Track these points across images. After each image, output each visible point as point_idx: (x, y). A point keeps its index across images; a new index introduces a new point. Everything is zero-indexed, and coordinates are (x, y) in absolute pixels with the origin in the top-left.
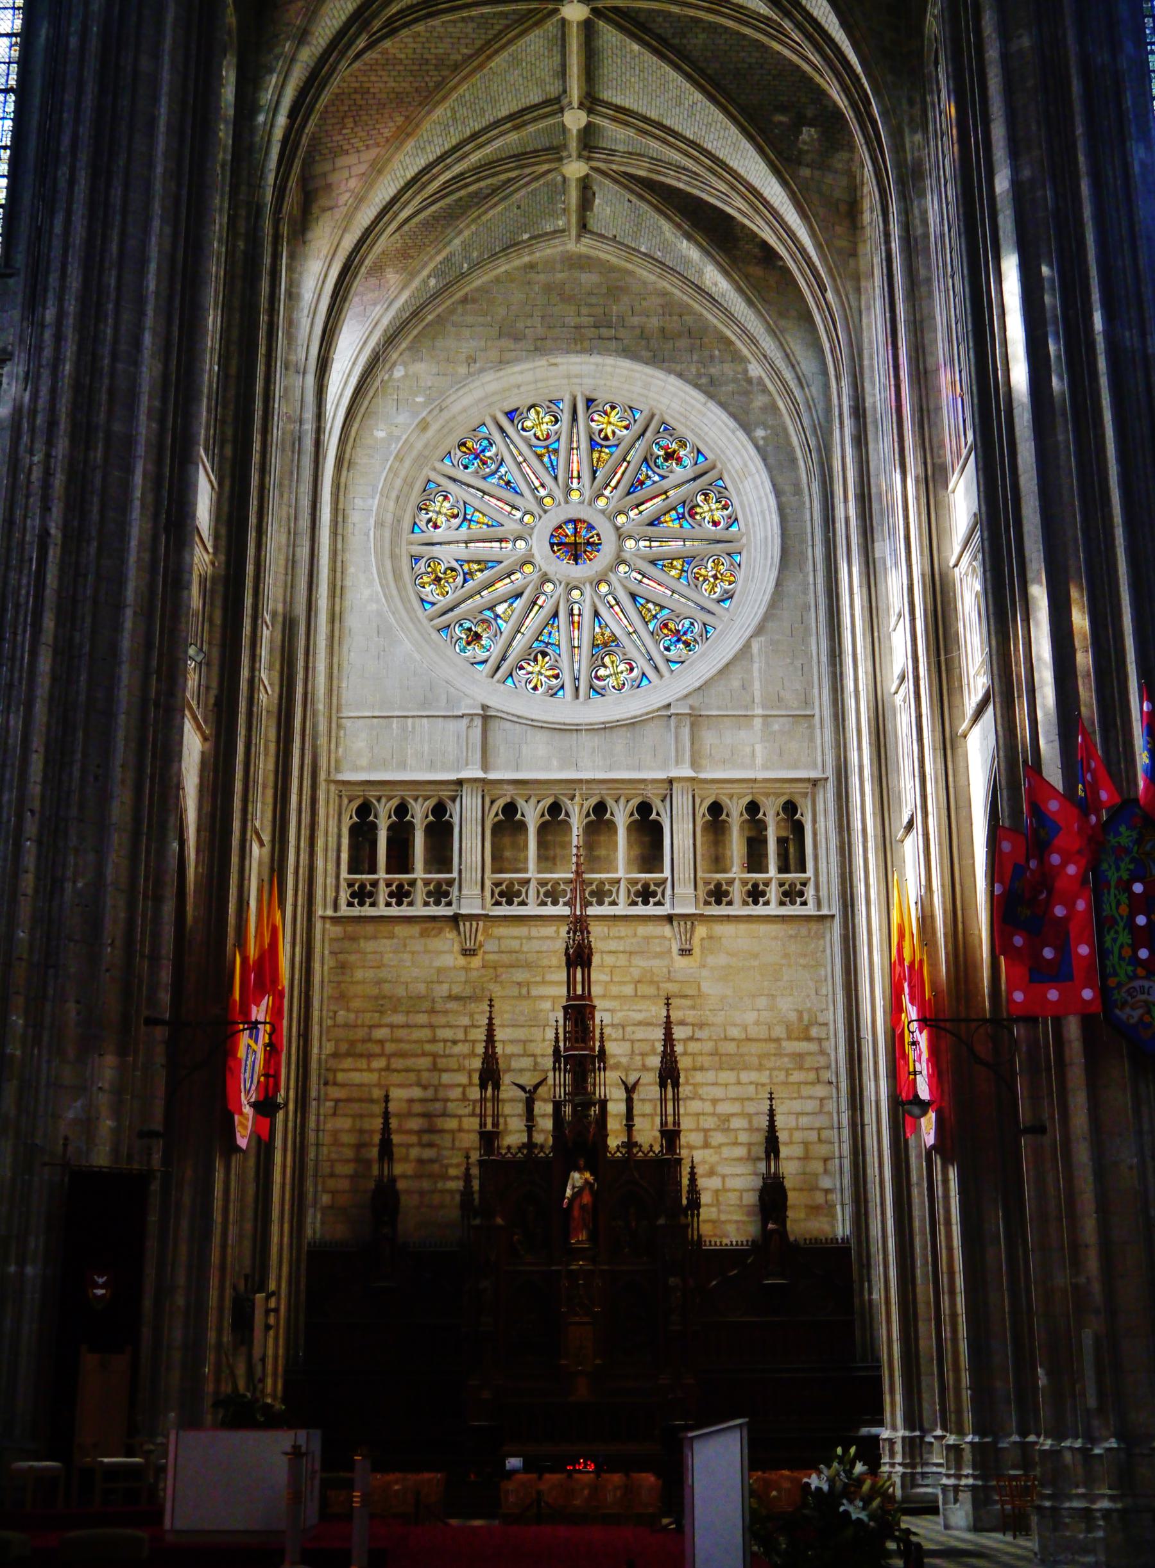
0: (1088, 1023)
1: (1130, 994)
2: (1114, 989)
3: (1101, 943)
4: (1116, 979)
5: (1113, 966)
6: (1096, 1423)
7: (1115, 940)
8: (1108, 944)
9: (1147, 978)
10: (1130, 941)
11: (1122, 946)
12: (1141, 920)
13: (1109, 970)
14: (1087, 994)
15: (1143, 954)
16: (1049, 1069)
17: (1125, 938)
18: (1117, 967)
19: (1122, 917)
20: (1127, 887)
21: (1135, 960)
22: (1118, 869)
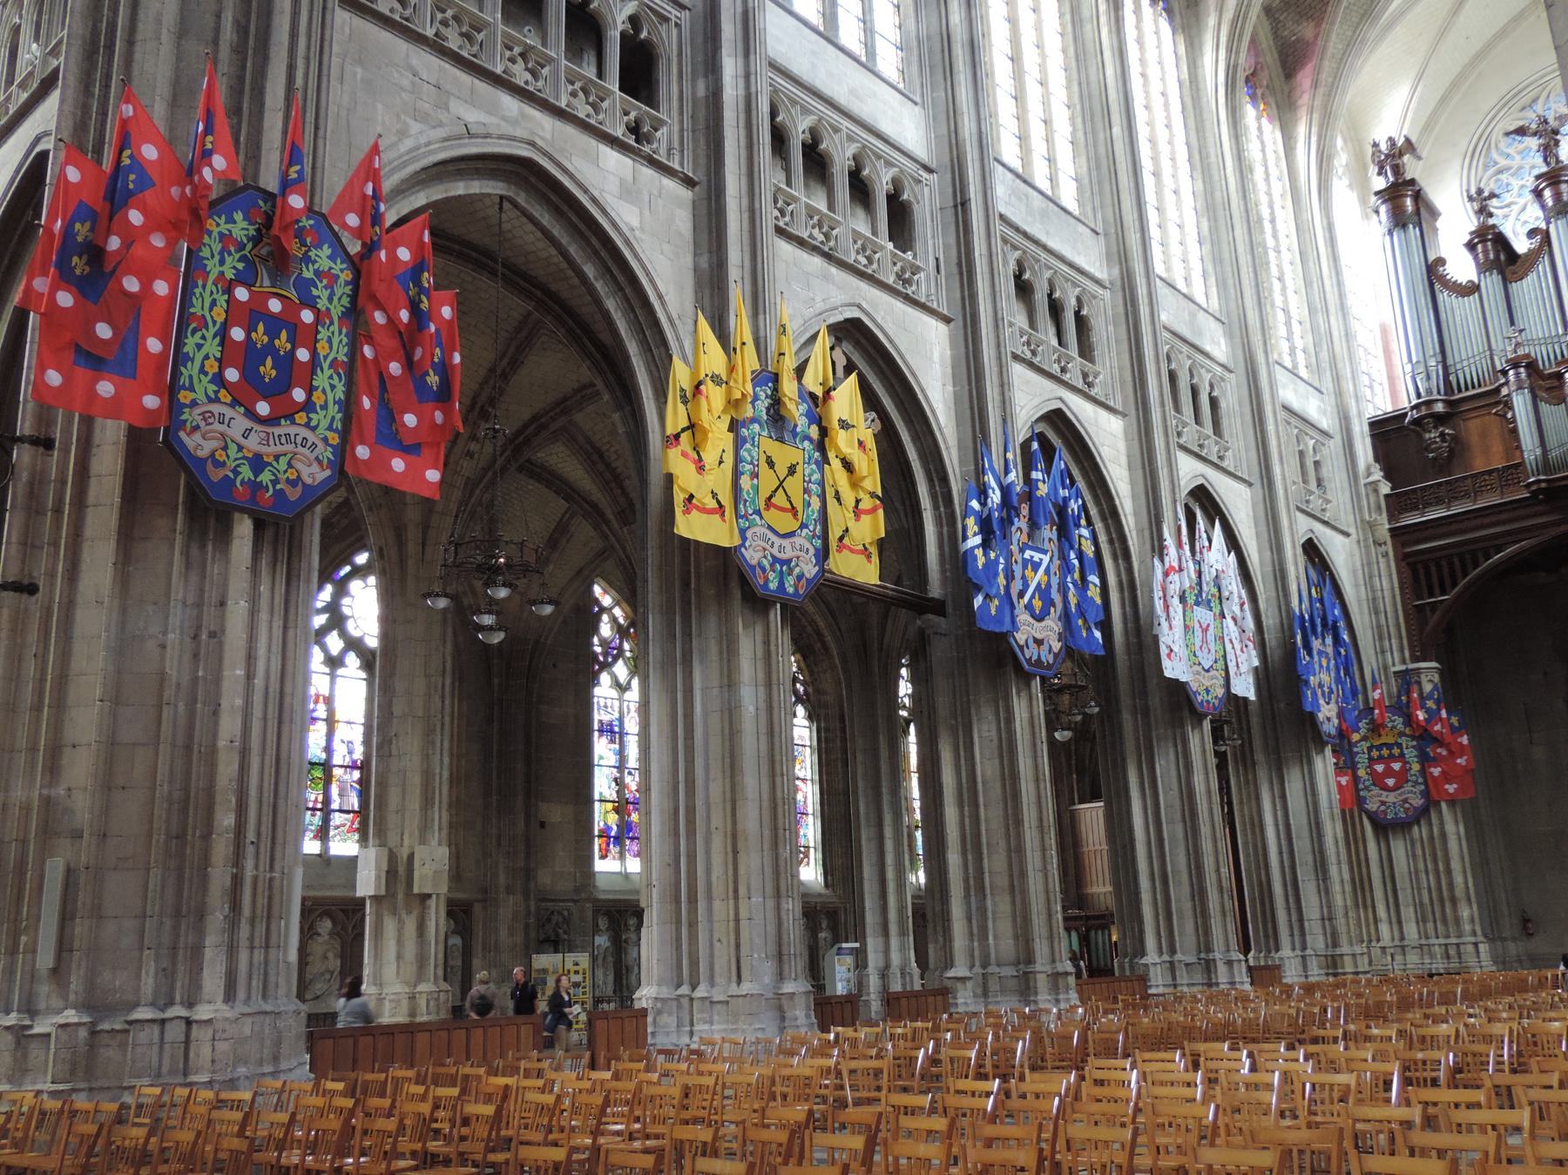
0: (138, 441)
1: (205, 419)
2: (185, 406)
3: (180, 344)
4: (191, 396)
5: (191, 377)
6: (44, 989)
7: (199, 347)
8: (189, 348)
9: (232, 405)
10: (218, 355)
11: (207, 357)
12: (237, 334)
13: (184, 380)
14: (151, 402)
15: (232, 375)
16: (58, 511)
17: (212, 347)
18: (195, 381)
19: (214, 323)
20: (229, 290)
21: (219, 379)
22: (222, 262)
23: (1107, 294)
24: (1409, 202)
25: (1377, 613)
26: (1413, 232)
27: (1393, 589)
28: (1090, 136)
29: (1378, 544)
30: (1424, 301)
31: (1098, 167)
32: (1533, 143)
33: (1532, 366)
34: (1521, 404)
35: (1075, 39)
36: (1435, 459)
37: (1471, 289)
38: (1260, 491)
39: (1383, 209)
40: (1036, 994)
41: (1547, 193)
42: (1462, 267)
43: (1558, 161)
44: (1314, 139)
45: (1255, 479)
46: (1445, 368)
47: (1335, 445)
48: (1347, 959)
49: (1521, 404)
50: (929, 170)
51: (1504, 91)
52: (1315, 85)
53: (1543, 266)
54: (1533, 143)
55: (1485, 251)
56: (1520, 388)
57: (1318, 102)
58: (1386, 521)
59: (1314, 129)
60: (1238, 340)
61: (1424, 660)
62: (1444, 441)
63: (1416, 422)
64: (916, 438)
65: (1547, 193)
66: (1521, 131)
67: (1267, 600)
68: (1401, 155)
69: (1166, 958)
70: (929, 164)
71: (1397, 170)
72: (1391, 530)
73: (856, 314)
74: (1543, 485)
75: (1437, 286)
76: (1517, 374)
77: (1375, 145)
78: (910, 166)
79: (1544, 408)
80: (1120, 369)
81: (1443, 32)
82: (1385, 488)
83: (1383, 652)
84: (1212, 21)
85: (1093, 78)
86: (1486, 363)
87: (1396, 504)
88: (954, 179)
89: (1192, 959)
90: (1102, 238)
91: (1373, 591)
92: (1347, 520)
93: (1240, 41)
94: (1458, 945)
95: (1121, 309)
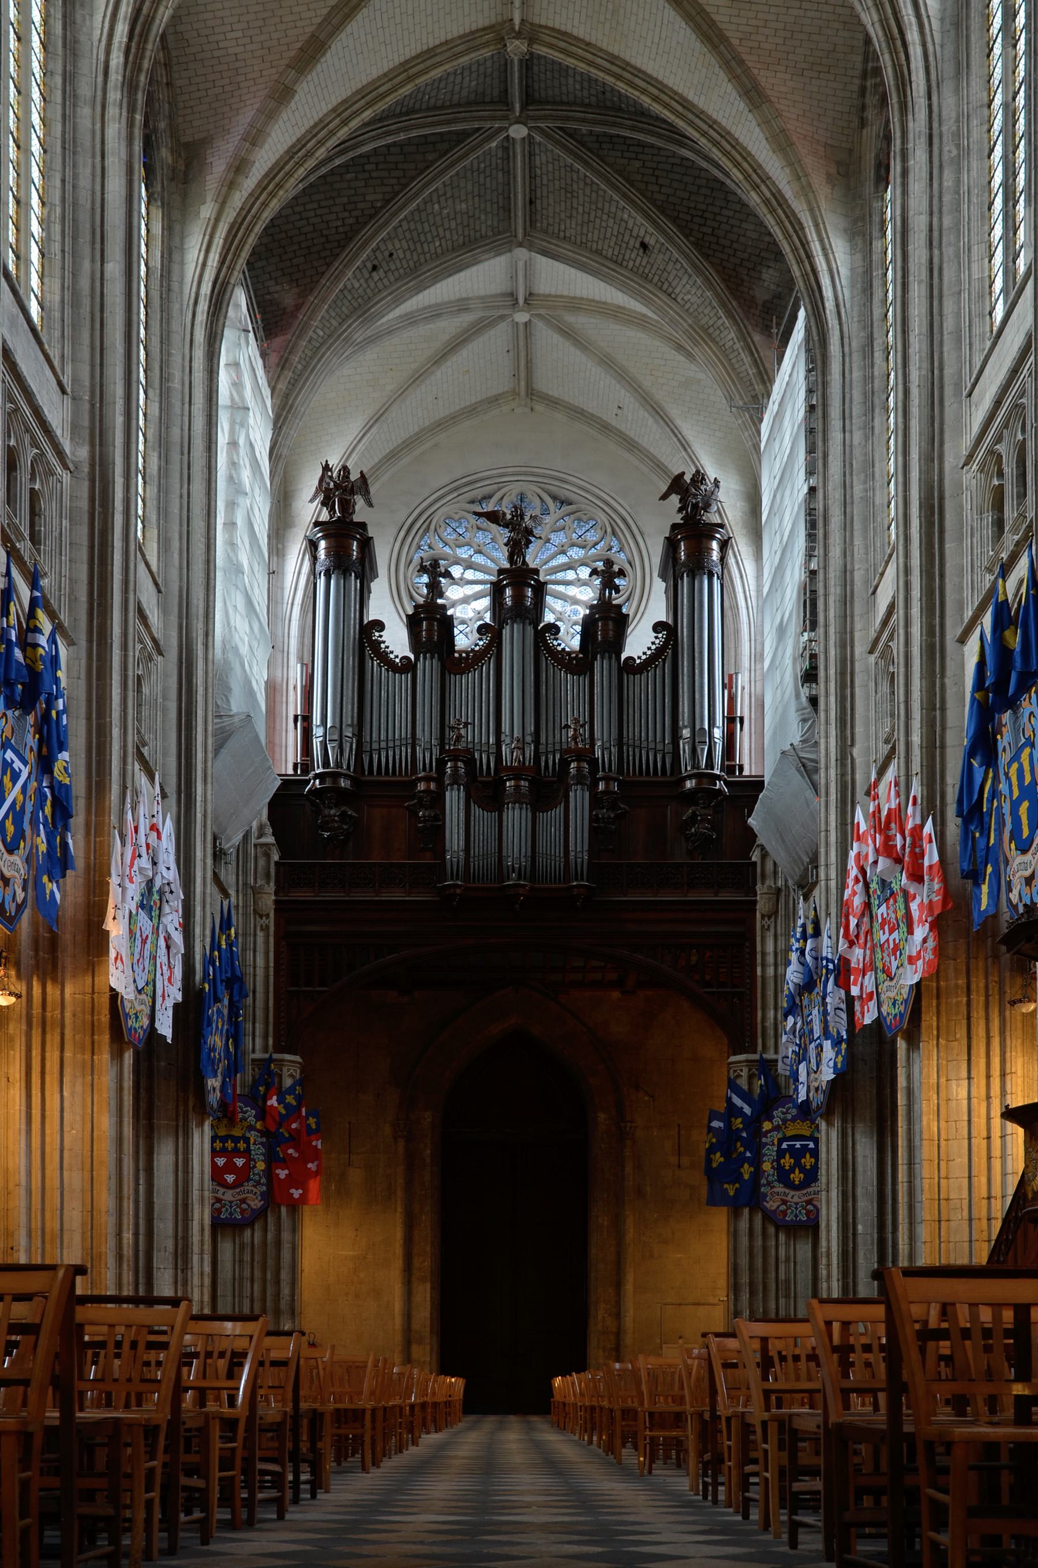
32: (504, 534)
41: (508, 592)
43: (524, 562)
65: (508, 592)
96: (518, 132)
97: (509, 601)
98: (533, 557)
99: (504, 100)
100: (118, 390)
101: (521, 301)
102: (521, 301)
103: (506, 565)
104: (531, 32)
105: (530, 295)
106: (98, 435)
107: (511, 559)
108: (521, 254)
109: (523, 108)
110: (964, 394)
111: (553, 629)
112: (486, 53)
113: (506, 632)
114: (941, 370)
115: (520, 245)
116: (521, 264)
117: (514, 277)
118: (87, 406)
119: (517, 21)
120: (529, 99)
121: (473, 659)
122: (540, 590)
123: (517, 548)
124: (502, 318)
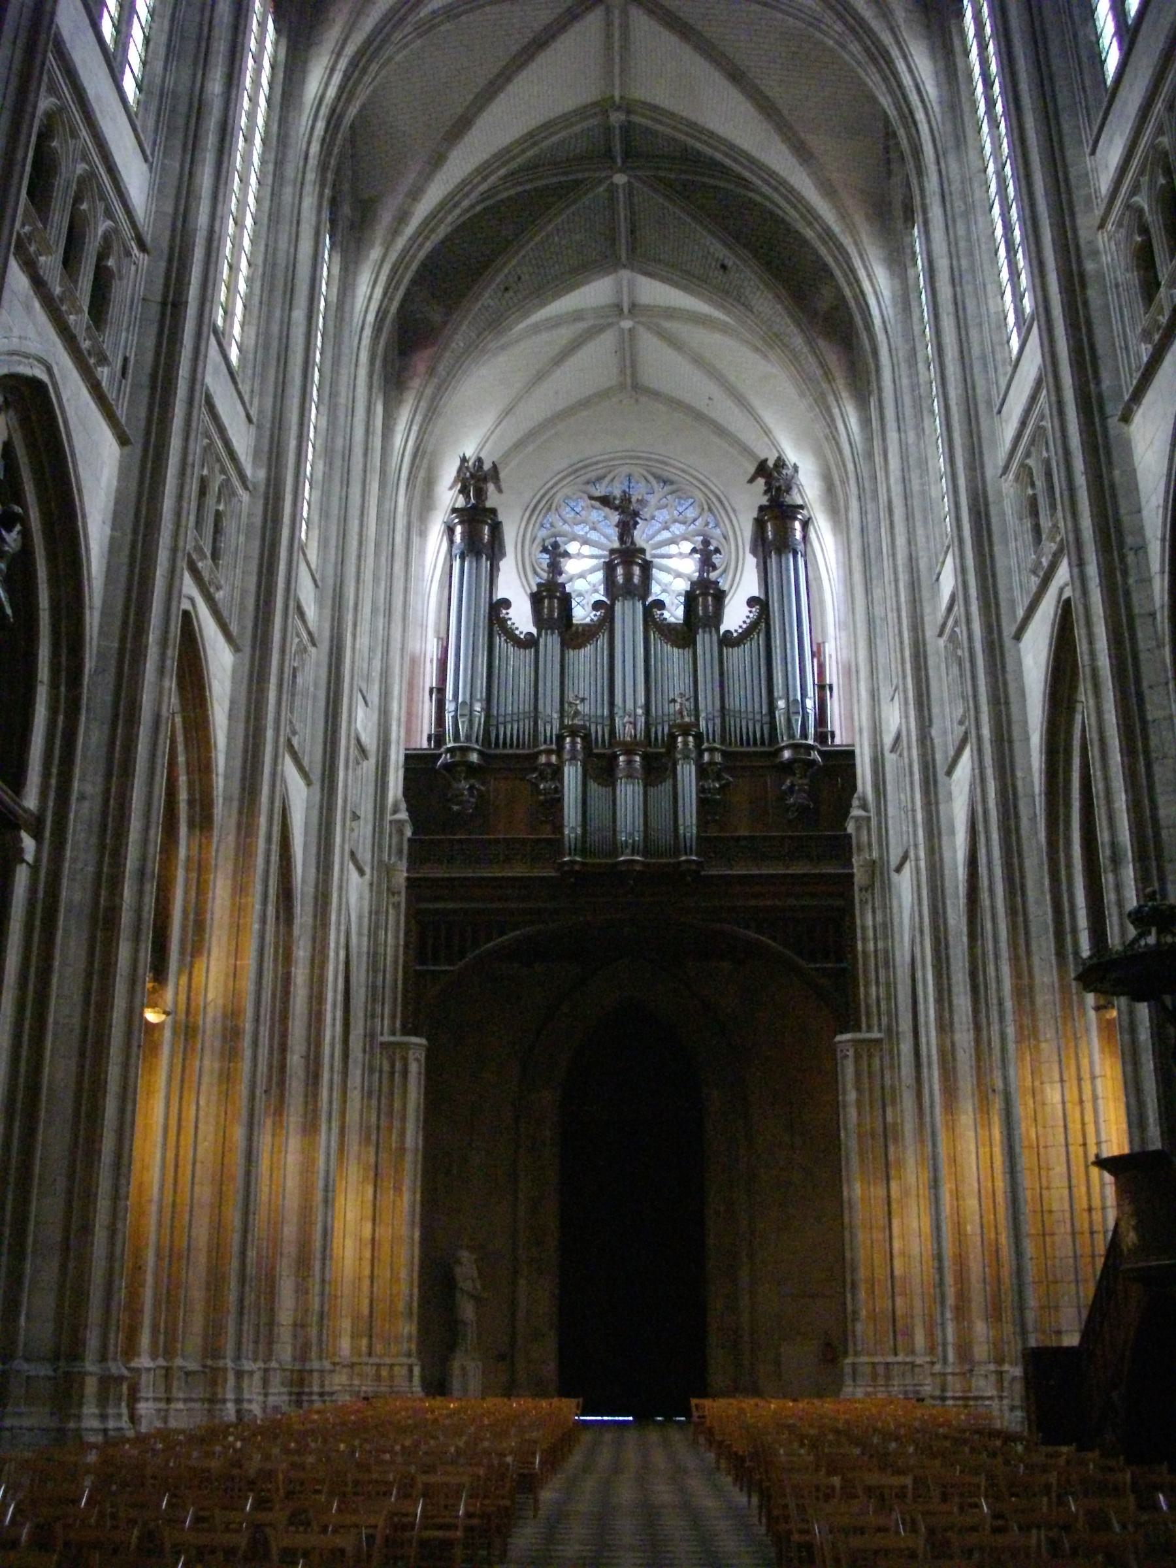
23: (245, 496)
24: (486, 529)
25: (375, 971)
26: (485, 564)
27: (397, 946)
28: (264, 308)
29: (392, 892)
30: (482, 640)
31: (266, 347)
32: (615, 517)
33: (586, 738)
34: (571, 775)
35: (272, 194)
36: (459, 813)
37: (530, 642)
38: (318, 797)
39: (458, 529)
40: (80, 1405)
42: (521, 618)
43: (633, 543)
44: (415, 428)
45: (316, 776)
46: (488, 716)
47: (369, 765)
48: (316, 1375)
49: (571, 775)
50: (142, 247)
51: (576, 458)
52: (431, 371)
53: (602, 640)
54: (615, 517)
55: (551, 610)
56: (573, 758)
57: (429, 391)
58: (403, 865)
59: (419, 418)
60: (328, 612)
61: (416, 1035)
62: (472, 795)
63: (446, 766)
64: (54, 581)
66: (605, 501)
67: (302, 926)
68: (485, 479)
69: (161, 1362)
70: (148, 239)
71: (480, 494)
72: (408, 879)
73: (45, 377)
74: (577, 867)
75: (496, 628)
76: (573, 743)
77: (464, 460)
78: (127, 231)
79: (593, 786)
80: (244, 592)
81: (540, 377)
82: (408, 833)
83: (373, 1016)
84: (375, 254)
85: (283, 244)
86: (527, 725)
87: (419, 852)
88: (168, 271)
89: (192, 1366)
90: (253, 429)
91: (376, 944)
92: (365, 856)
93: (396, 288)
94: (392, 1365)
95: (258, 521)
96: (620, 179)
97: (620, 579)
98: (641, 536)
99: (609, 154)
100: (294, 418)
101: (626, 310)
102: (626, 310)
103: (616, 545)
104: (628, 107)
105: (633, 306)
106: (273, 454)
107: (621, 539)
108: (625, 274)
109: (624, 162)
110: (995, 410)
111: (660, 604)
112: (593, 122)
113: (618, 607)
114: (974, 388)
115: (624, 266)
116: (625, 283)
117: (619, 292)
118: (268, 433)
119: (617, 98)
120: (627, 155)
121: (586, 635)
122: (647, 567)
123: (626, 529)
124: (610, 325)
